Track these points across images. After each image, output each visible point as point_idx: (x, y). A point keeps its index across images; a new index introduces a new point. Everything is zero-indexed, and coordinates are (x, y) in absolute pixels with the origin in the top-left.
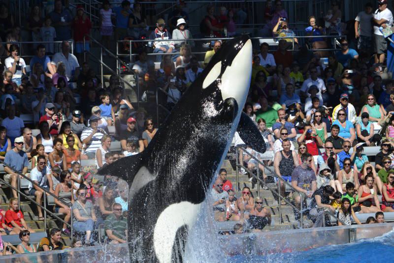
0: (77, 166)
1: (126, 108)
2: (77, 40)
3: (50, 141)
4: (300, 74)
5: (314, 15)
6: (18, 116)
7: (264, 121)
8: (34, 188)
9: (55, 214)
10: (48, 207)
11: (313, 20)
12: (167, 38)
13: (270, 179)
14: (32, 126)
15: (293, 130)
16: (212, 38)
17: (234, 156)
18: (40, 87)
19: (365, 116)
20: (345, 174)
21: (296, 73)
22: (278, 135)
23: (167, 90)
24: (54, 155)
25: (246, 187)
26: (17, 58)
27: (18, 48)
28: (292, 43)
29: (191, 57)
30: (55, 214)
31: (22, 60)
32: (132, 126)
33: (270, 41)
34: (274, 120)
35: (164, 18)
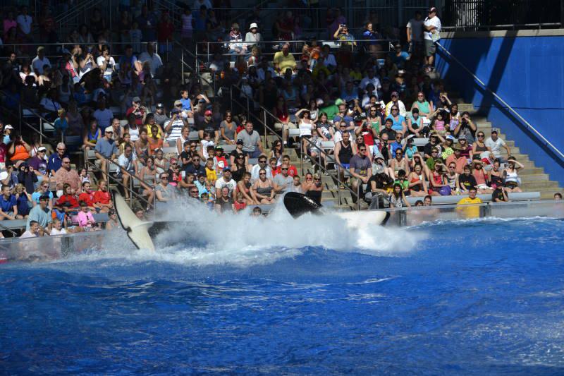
0: (159, 153)
1: (204, 101)
2: (161, 40)
3: (136, 131)
4: (360, 74)
5: (371, 21)
6: (108, 108)
7: (326, 115)
8: (121, 172)
9: (139, 195)
10: (133, 189)
11: (370, 25)
13: (331, 166)
14: (120, 118)
15: (352, 123)
16: (280, 41)
17: (299, 145)
18: (127, 82)
19: (416, 111)
20: (397, 163)
21: (356, 72)
22: (338, 127)
23: (240, 87)
24: (140, 143)
25: (309, 173)
26: (107, 57)
27: (108, 48)
28: (351, 46)
29: (261, 58)
30: (139, 195)
31: (112, 59)
32: (209, 118)
33: (331, 44)
34: (335, 114)
35: (236, 21)
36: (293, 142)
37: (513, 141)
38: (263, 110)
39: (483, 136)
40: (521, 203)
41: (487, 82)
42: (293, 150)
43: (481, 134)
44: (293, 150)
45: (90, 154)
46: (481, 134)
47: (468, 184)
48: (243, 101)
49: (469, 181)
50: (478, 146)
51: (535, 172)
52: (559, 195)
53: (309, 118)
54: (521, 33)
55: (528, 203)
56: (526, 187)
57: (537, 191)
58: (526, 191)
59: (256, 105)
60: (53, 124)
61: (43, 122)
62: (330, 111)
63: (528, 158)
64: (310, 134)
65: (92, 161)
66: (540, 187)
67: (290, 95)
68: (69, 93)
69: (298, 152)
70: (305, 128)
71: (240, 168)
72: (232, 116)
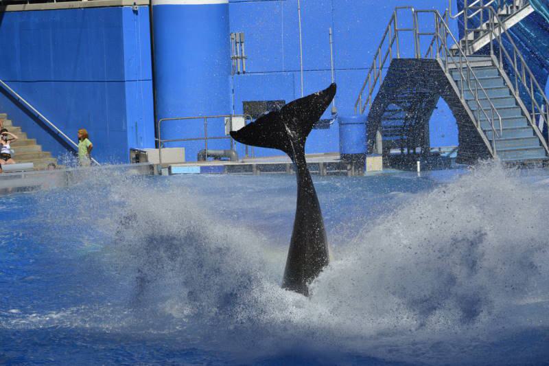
37: (5, 114)
40: (15, 174)
51: (27, 143)
52: (54, 165)
54: (10, 8)
55: (22, 174)
56: (19, 158)
57: (31, 162)
58: (20, 162)
63: (20, 130)
66: (33, 158)
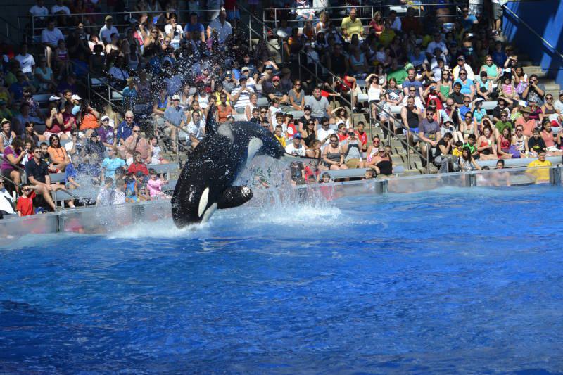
1: (272, 68)
3: (206, 99)
7: (395, 80)
8: (190, 140)
12: (308, 6)
17: (367, 110)
19: (484, 74)
26: (174, 25)
28: (418, 10)
32: (276, 84)
33: (398, 9)
34: (403, 78)
36: (361, 106)
38: (332, 76)
39: (551, 98)
41: (555, 44)
42: (362, 115)
43: (549, 97)
44: (362, 115)
45: (158, 121)
46: (549, 97)
47: (537, 147)
48: (312, 66)
49: (537, 144)
50: (547, 109)
53: (377, 83)
59: (324, 70)
60: (122, 92)
61: (112, 90)
62: (398, 75)
64: (379, 99)
65: (161, 129)
67: (358, 60)
68: (138, 62)
69: (367, 116)
70: (374, 93)
71: (310, 133)
72: (301, 84)
